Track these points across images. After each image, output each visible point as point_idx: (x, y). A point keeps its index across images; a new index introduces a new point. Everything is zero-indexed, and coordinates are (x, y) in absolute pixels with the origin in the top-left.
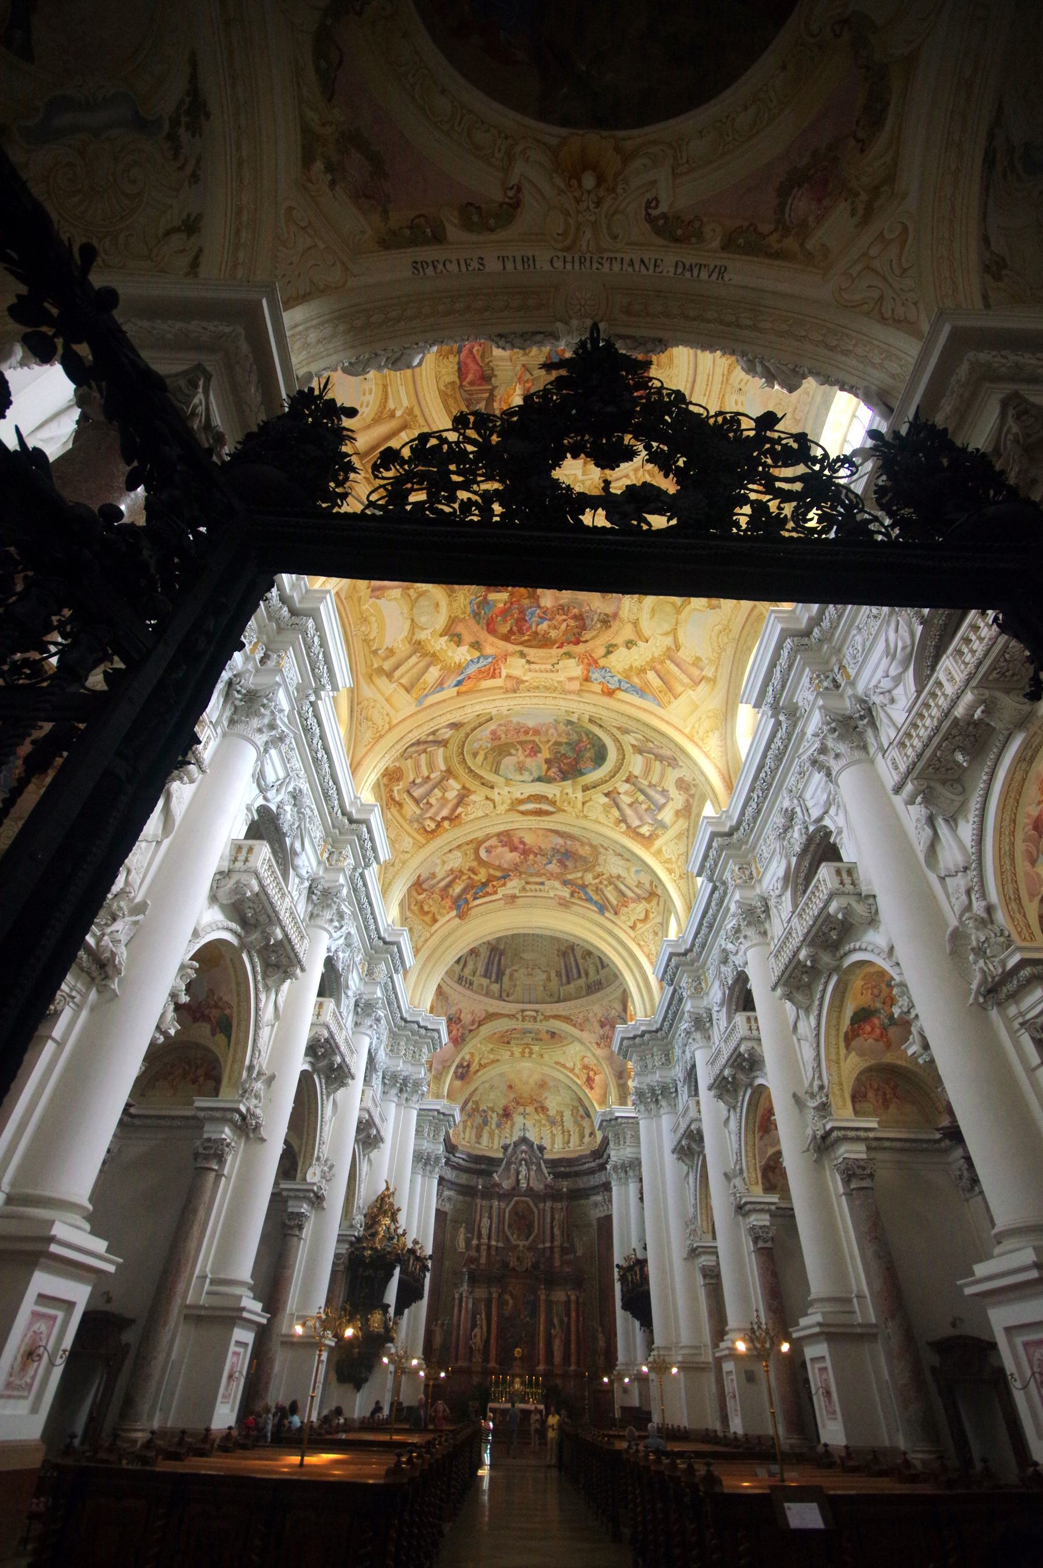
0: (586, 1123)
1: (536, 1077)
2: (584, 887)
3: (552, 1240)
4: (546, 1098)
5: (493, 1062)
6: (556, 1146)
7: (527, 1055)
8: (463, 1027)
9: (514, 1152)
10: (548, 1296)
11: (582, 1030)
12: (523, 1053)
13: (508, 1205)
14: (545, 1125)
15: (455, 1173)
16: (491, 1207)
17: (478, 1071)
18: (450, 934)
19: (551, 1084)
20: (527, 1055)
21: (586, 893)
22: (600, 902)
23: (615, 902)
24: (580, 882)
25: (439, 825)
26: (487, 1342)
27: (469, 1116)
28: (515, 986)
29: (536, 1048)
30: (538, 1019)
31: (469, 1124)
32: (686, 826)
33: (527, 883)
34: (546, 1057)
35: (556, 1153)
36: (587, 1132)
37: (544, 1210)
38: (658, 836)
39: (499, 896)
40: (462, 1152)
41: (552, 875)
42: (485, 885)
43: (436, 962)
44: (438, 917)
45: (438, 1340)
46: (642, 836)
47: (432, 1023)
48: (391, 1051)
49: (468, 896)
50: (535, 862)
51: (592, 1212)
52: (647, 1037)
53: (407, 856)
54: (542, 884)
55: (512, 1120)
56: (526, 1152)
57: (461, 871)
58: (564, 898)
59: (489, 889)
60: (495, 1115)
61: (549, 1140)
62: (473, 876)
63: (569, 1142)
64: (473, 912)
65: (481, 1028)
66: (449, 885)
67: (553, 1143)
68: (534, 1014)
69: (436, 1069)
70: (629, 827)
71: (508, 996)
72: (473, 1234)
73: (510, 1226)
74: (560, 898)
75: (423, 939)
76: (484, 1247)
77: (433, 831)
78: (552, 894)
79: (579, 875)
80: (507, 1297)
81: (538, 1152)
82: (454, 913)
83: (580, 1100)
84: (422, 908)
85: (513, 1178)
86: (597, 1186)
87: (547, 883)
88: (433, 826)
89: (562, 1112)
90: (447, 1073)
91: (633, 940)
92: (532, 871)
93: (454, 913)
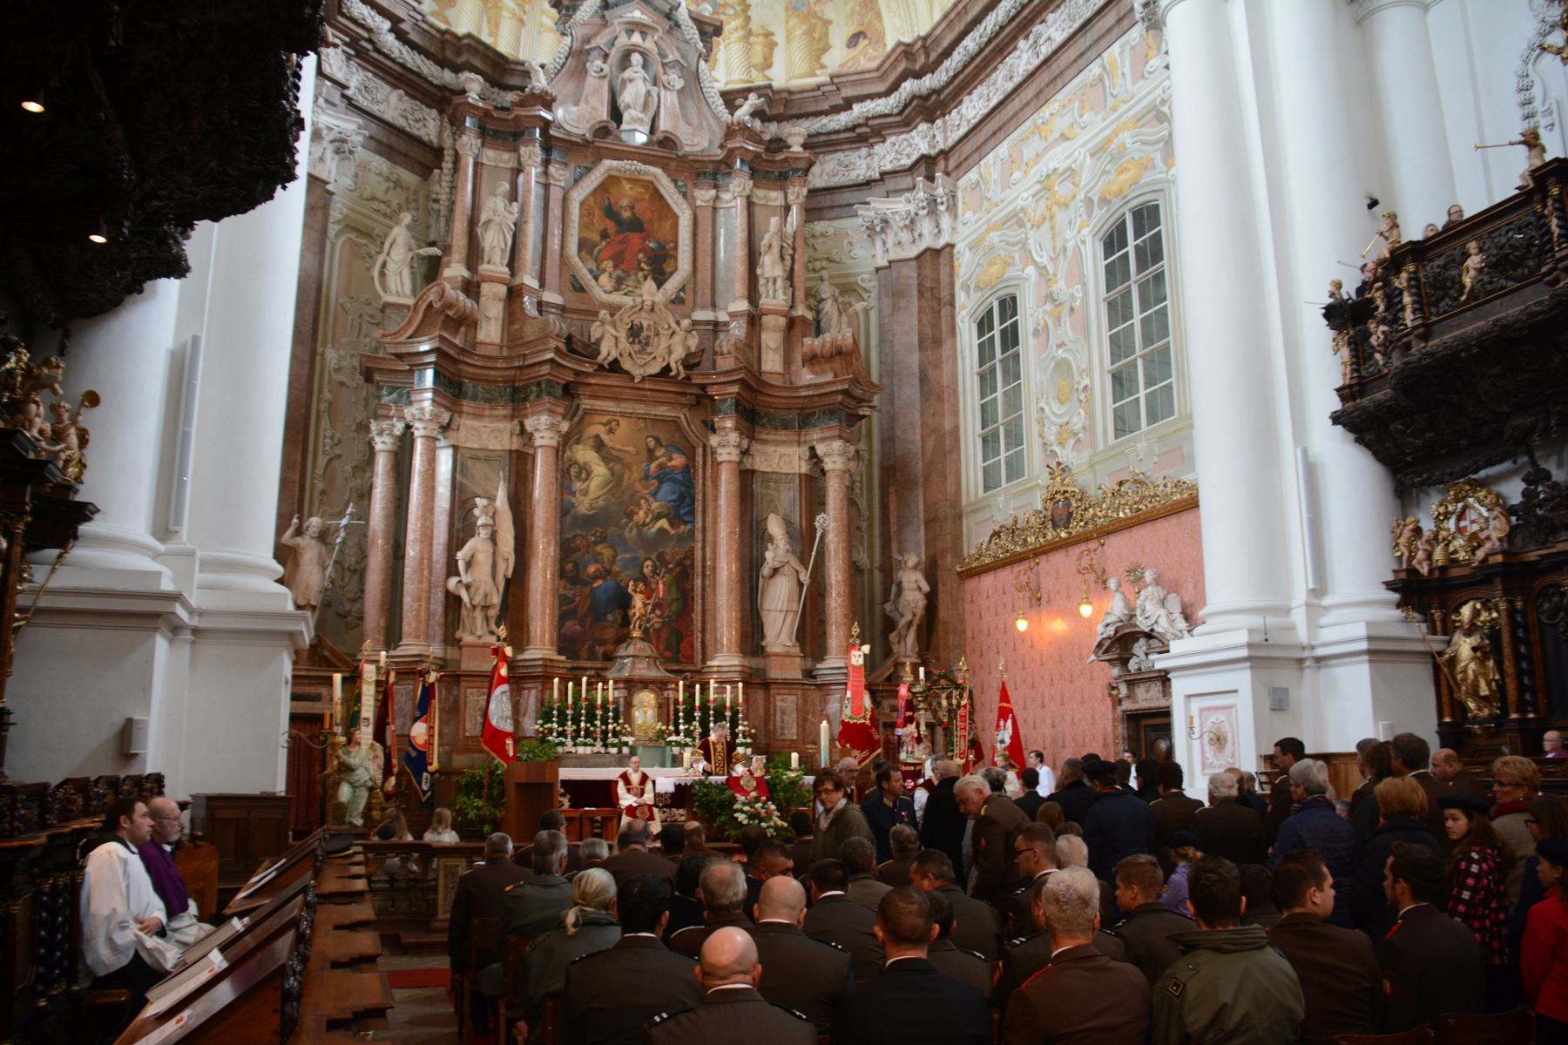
3: (753, 294)
10: (745, 453)
13: (576, 181)
16: (518, 171)
26: (516, 586)
37: (715, 209)
45: (366, 502)
51: (859, 252)
56: (644, 29)
63: (767, 64)
72: (447, 249)
73: (583, 244)
76: (494, 294)
80: (584, 454)
81: (692, 32)
86: (883, 175)
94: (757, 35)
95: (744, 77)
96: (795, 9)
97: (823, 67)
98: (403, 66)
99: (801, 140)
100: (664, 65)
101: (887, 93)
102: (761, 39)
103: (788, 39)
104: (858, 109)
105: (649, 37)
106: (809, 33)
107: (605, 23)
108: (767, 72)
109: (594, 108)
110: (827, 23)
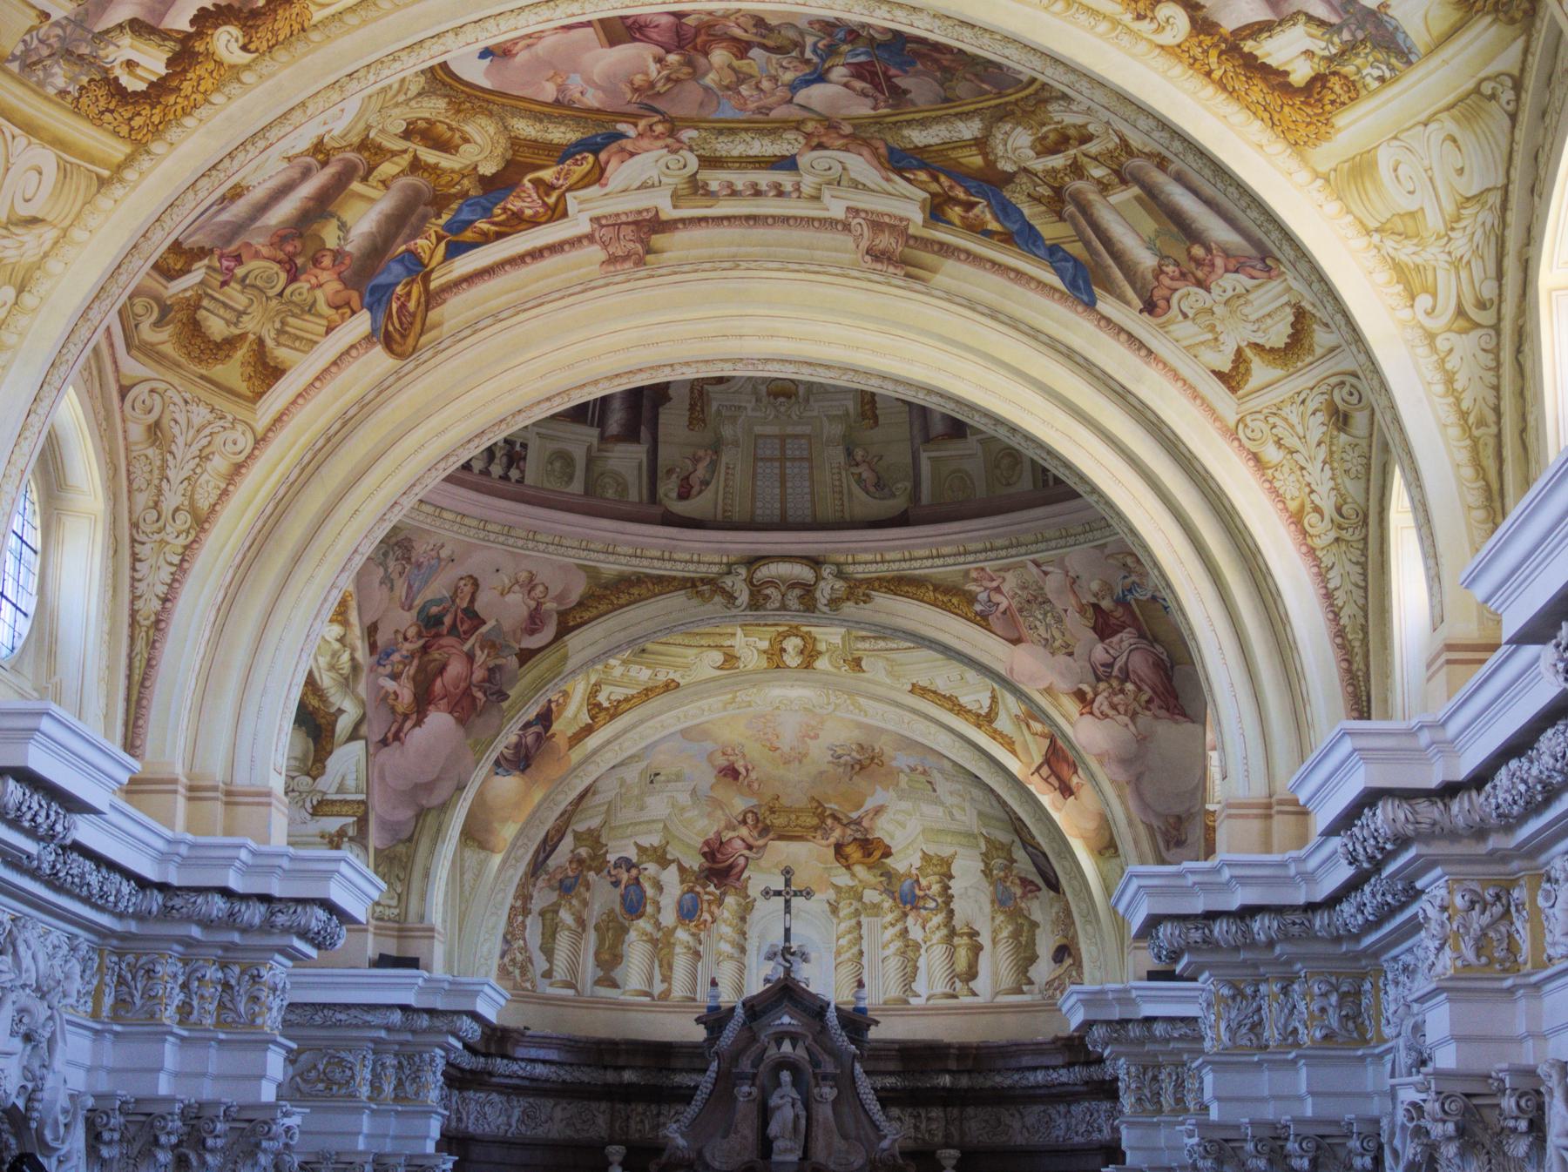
0: (1040, 909)
1: (839, 732)
2: (992, 183)
4: (878, 811)
5: (648, 693)
6: (920, 986)
7: (792, 659)
8: (491, 645)
9: (750, 1033)
11: (1016, 641)
12: (775, 656)
14: (876, 908)
15: (518, 1107)
17: (588, 730)
18: (348, 423)
19: (902, 760)
20: (792, 659)
21: (1005, 210)
22: (1076, 249)
23: (1146, 260)
24: (978, 161)
25: (185, 54)
27: (566, 888)
28: (716, 447)
29: (829, 636)
30: (824, 593)
31: (565, 916)
32: (1508, 60)
33: (711, 162)
34: (875, 669)
35: (922, 1012)
36: (1046, 945)
38: (1354, 89)
39: (577, 223)
40: (544, 1042)
41: (831, 125)
42: (498, 185)
43: (297, 559)
44: (282, 354)
46: (1275, 78)
47: (289, 874)
48: (121, 1003)
49: (422, 244)
50: (742, 78)
52: (1261, 927)
53: (32, 243)
54: (787, 163)
55: (743, 892)
56: (795, 1038)
57: (364, 145)
58: (898, 228)
59: (525, 201)
60: (670, 876)
61: (894, 963)
62: (430, 156)
63: (971, 974)
64: (453, 311)
65: (576, 642)
66: (323, 206)
67: (909, 975)
68: (803, 572)
69: (384, 825)
70: (1203, 25)
71: (684, 495)
74: (877, 226)
75: (219, 464)
77: (158, 90)
78: (837, 210)
79: (969, 130)
81: (842, 1039)
82: (361, 323)
83: (1017, 826)
84: (193, 330)
85: (747, 1130)
87: (804, 161)
88: (153, 61)
89: (946, 863)
90: (438, 835)
91: (1232, 435)
92: (728, 111)
93: (361, 323)
94: (962, 935)
95: (947, 990)
96: (1002, 903)
97: (1030, 982)
98: (564, 1081)
99: (954, 1162)
100: (815, 1075)
101: (1069, 1065)
102: (965, 940)
103: (994, 942)
104: (1040, 1076)
105: (800, 1043)
106: (1016, 935)
107: (754, 1039)
108: (972, 984)
109: (745, 1138)
110: (1034, 925)
